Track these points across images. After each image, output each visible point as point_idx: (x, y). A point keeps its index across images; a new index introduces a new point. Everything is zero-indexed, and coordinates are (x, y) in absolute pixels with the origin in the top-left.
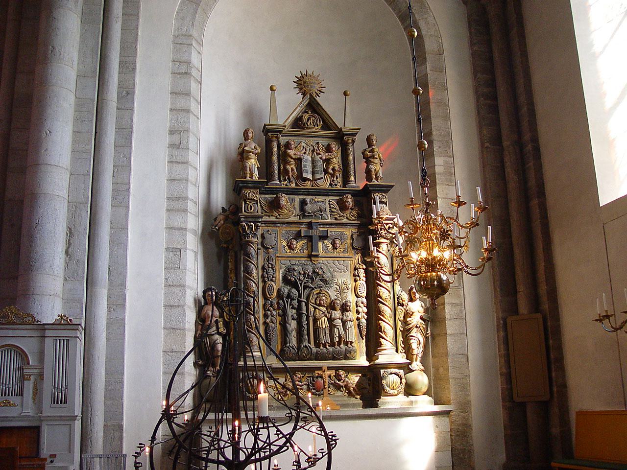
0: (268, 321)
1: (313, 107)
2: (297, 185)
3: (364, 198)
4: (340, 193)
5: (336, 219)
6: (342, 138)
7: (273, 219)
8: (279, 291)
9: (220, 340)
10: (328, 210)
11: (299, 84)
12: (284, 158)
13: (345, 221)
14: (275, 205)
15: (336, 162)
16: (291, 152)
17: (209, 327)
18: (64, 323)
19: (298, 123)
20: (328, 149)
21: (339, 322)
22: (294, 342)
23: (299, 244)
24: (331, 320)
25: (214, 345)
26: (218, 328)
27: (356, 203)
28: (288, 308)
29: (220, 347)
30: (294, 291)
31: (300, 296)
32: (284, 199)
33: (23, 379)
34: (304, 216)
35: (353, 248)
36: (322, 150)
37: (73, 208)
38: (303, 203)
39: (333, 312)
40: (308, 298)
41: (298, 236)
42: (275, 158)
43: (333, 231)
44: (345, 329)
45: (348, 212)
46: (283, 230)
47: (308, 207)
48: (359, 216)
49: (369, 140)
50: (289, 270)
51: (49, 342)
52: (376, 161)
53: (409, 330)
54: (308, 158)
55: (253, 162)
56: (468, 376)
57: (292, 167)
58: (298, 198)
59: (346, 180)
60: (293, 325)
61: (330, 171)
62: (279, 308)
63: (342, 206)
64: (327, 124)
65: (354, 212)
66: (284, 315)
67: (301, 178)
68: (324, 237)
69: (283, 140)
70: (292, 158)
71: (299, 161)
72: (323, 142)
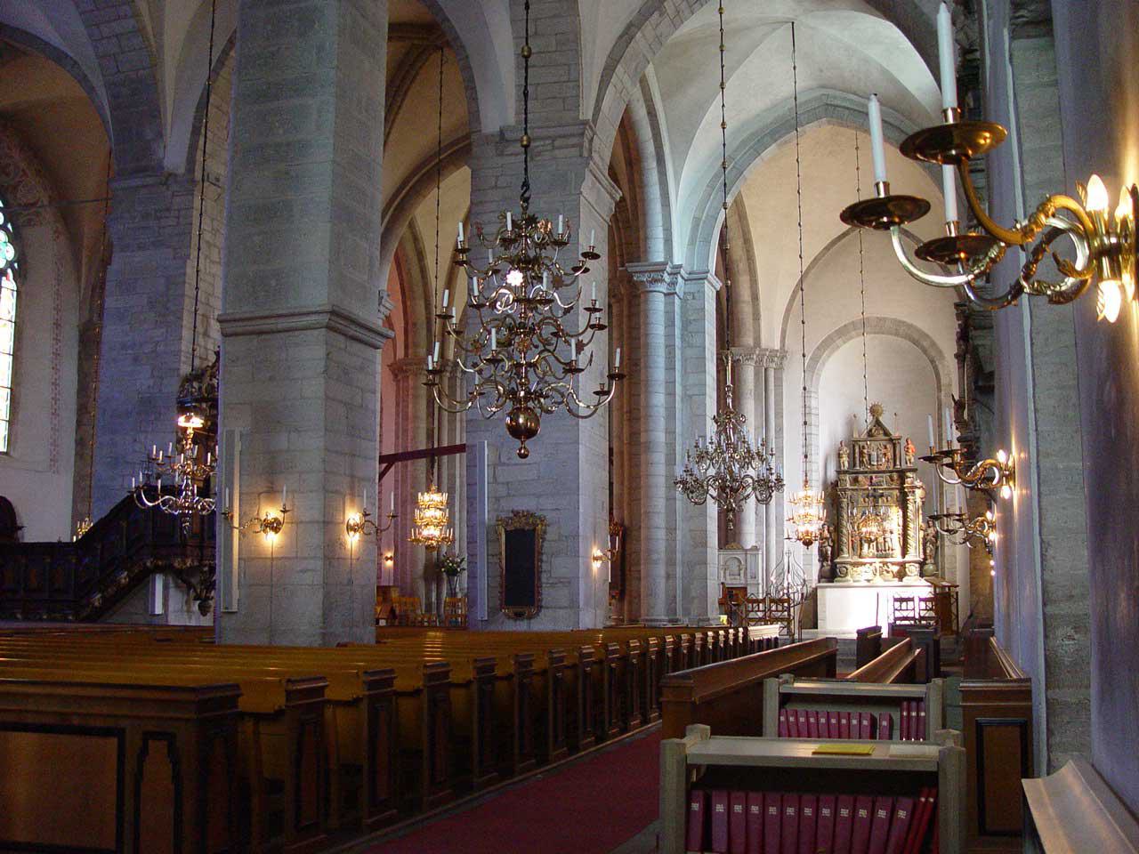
1: (878, 423)
3: (902, 475)
4: (891, 472)
6: (893, 442)
7: (856, 487)
9: (829, 549)
12: (861, 453)
14: (856, 481)
15: (890, 455)
16: (865, 451)
18: (756, 548)
19: (870, 434)
25: (827, 551)
29: (829, 552)
32: (861, 477)
33: (740, 570)
36: (882, 448)
37: (769, 392)
38: (871, 478)
47: (874, 480)
51: (748, 556)
53: (926, 543)
54: (874, 454)
55: (845, 459)
56: (955, 568)
57: (865, 459)
64: (886, 433)
68: (882, 495)
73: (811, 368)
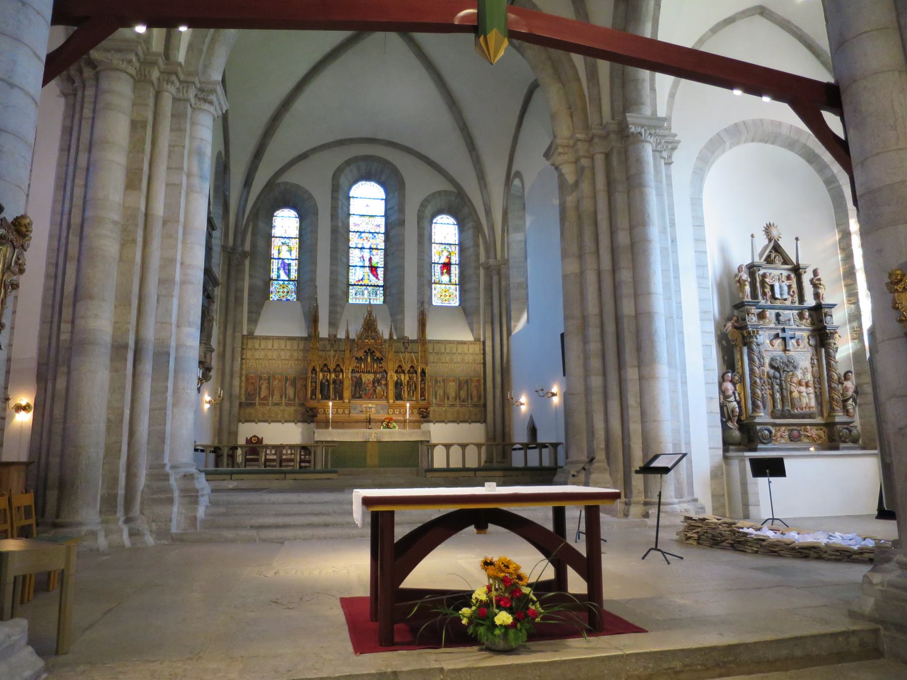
0: (763, 393)
1: (777, 249)
2: (771, 303)
5: (798, 326)
8: (768, 373)
10: (792, 320)
11: (766, 229)
12: (763, 283)
13: (803, 327)
15: (794, 286)
16: (767, 280)
17: (729, 397)
19: (769, 260)
20: (788, 278)
21: (805, 394)
22: (779, 407)
23: (778, 342)
24: (800, 392)
26: (735, 397)
27: (810, 315)
28: (775, 384)
30: (777, 374)
31: (781, 377)
34: (779, 323)
35: (809, 345)
39: (800, 387)
40: (786, 378)
41: (777, 336)
42: (758, 284)
43: (798, 334)
44: (810, 399)
45: (805, 320)
46: (767, 333)
47: (781, 318)
48: (812, 324)
49: (815, 273)
50: (772, 359)
52: (821, 287)
57: (768, 290)
58: (774, 312)
59: (801, 299)
60: (778, 396)
61: (791, 293)
62: (769, 385)
63: (801, 316)
64: (786, 261)
65: (809, 321)
66: (772, 388)
67: (773, 297)
69: (762, 272)
70: (768, 284)
71: (772, 287)
72: (785, 273)
73: (699, 174)
